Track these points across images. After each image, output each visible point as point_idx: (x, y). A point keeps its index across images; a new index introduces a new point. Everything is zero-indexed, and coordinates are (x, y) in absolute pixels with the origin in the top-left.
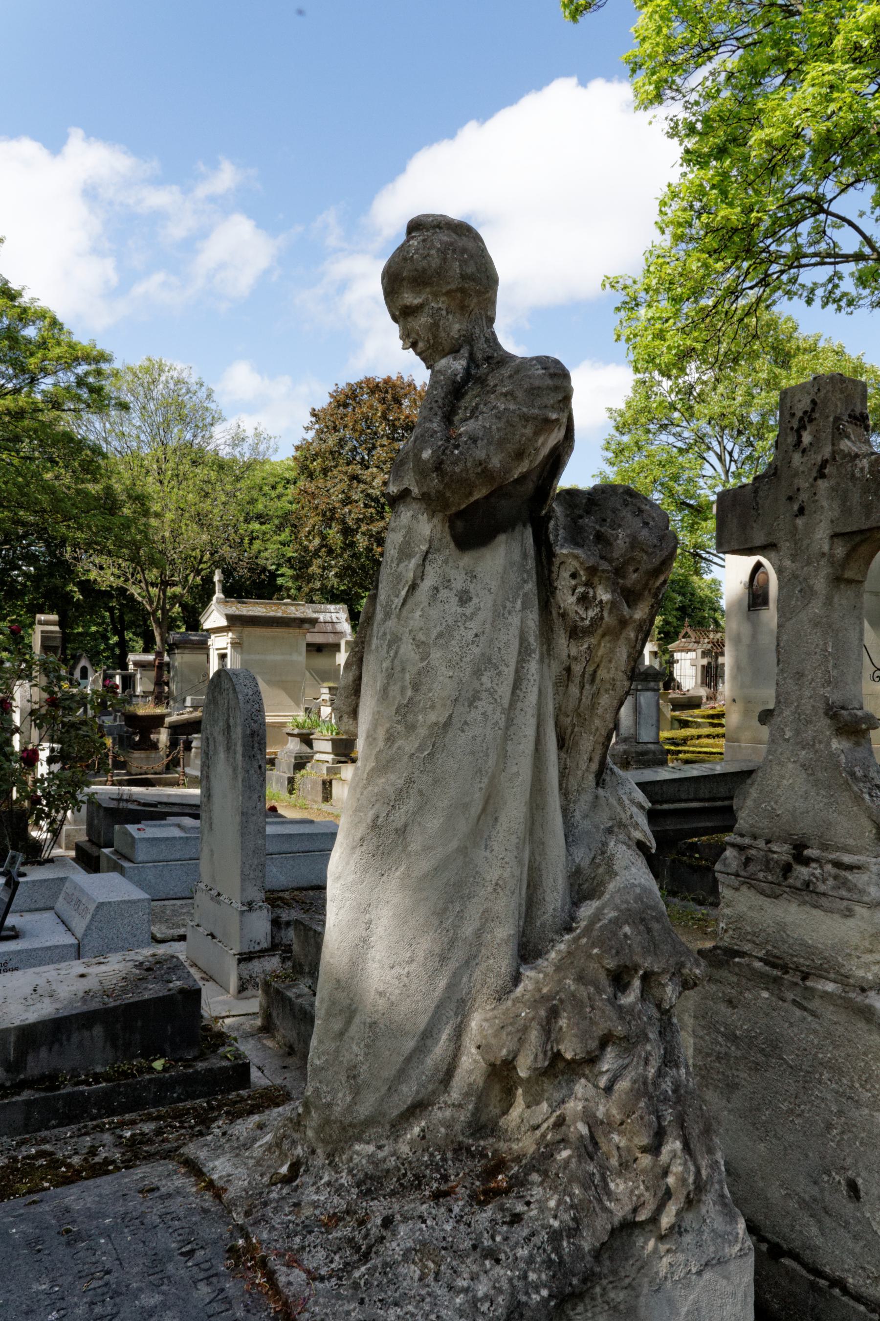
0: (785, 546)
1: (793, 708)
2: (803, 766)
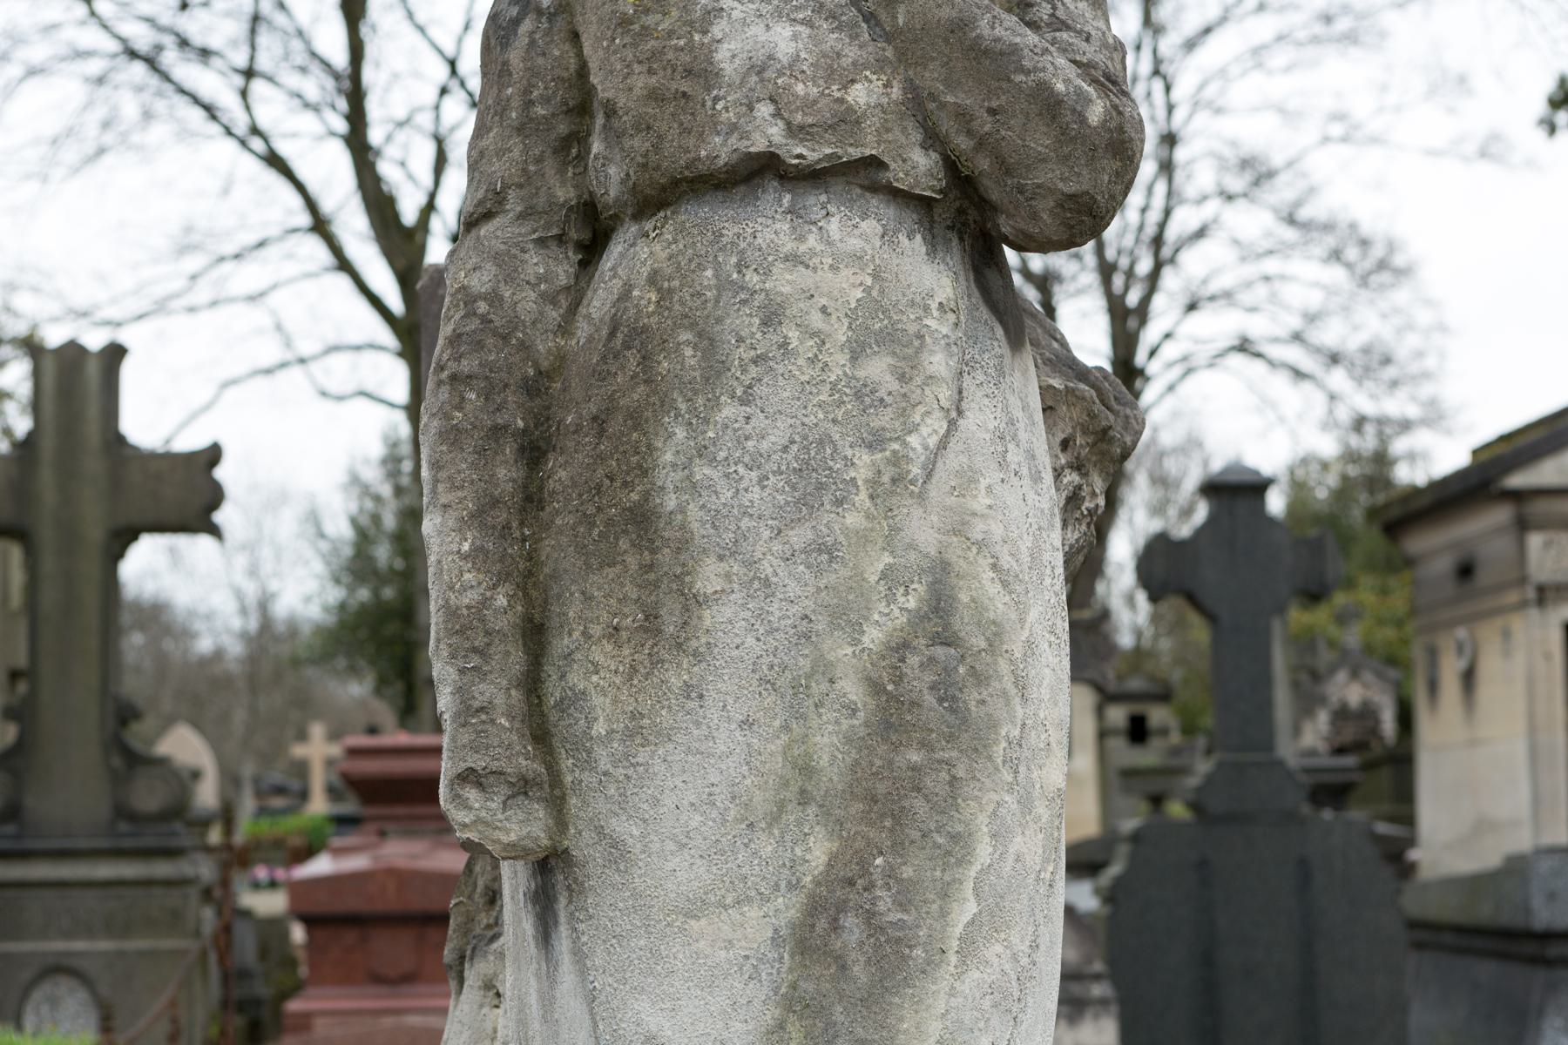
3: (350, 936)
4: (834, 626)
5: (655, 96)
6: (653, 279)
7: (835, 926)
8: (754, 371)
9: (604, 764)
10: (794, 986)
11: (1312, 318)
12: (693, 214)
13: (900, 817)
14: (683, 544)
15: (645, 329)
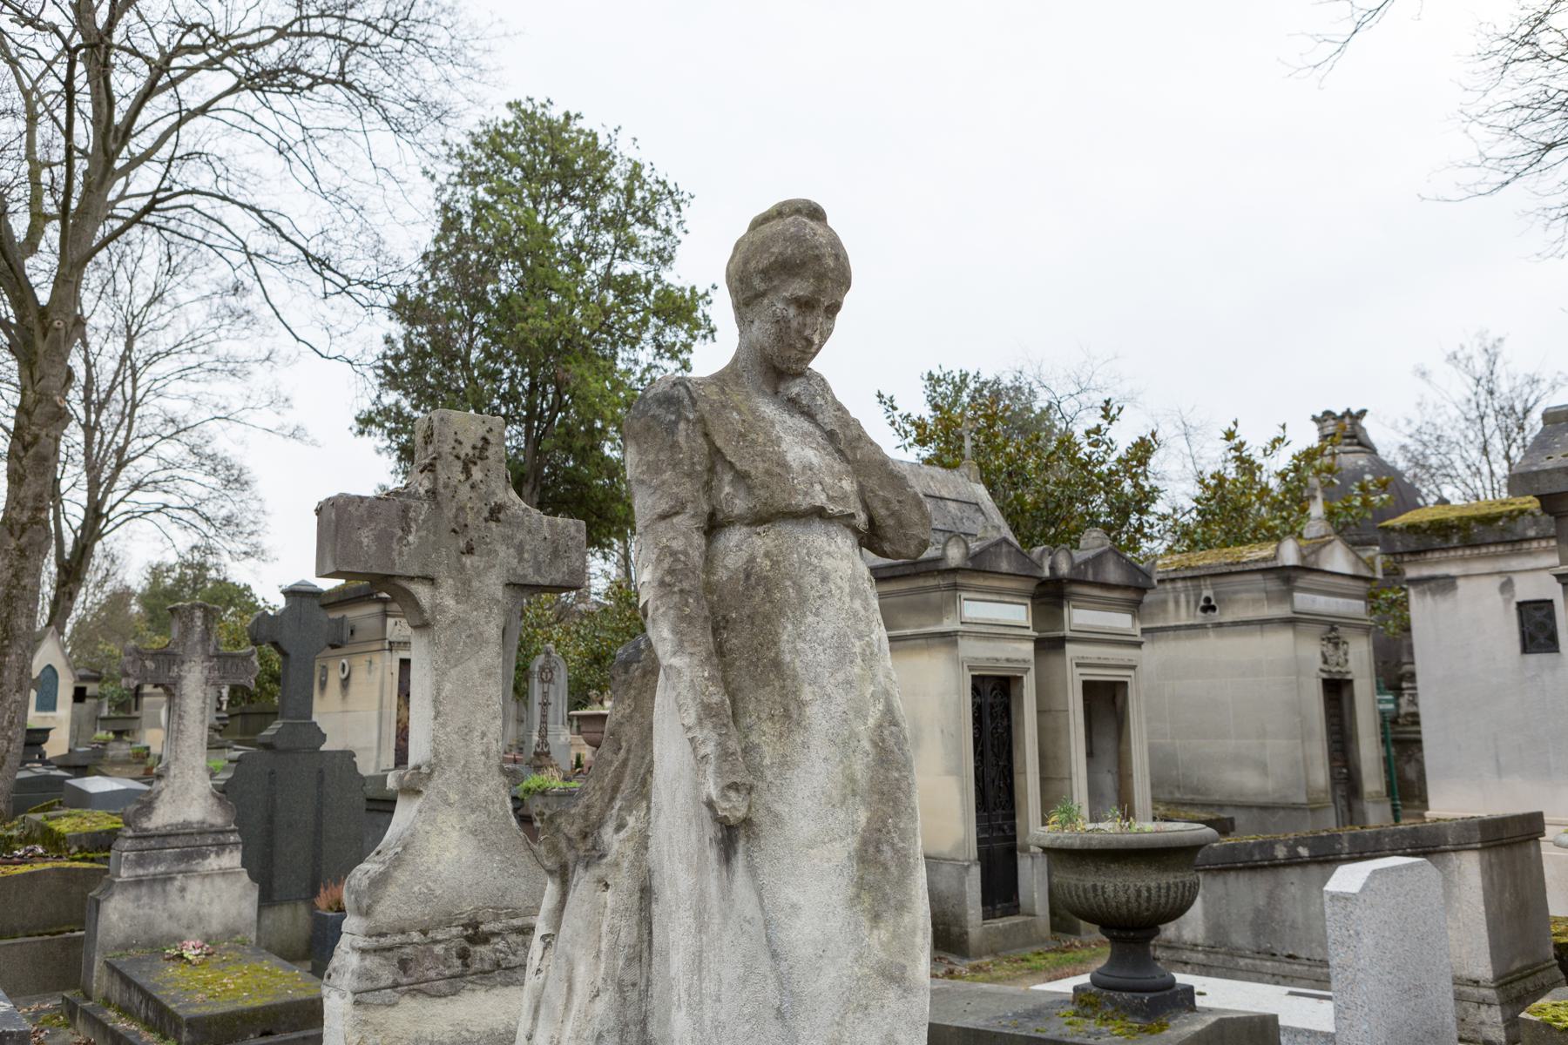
0: (447, 584)
1: (459, 767)
2: (474, 833)
4: (856, 717)
5: (768, 472)
6: (767, 555)
7: (878, 851)
8: (819, 602)
9: (770, 778)
10: (862, 878)
11: (202, 501)
12: (787, 528)
13: (896, 801)
14: (795, 677)
15: (766, 577)
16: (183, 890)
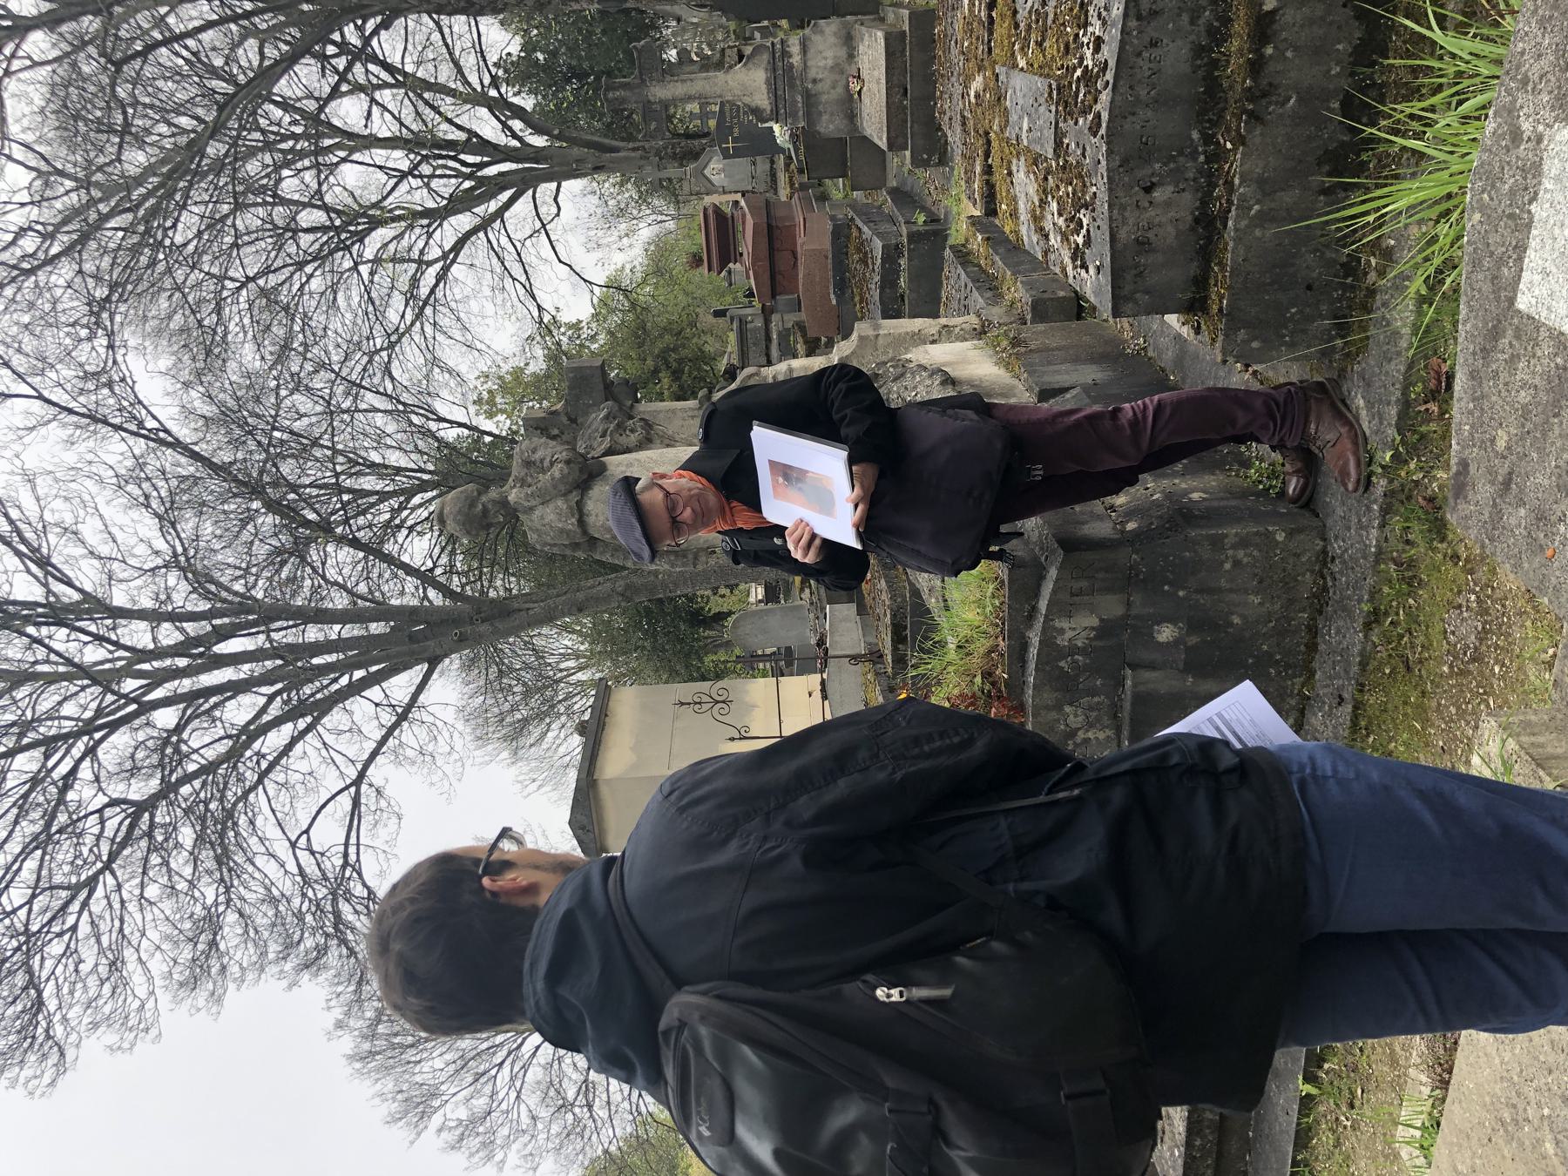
3: (779, 277)
16: (814, 81)
